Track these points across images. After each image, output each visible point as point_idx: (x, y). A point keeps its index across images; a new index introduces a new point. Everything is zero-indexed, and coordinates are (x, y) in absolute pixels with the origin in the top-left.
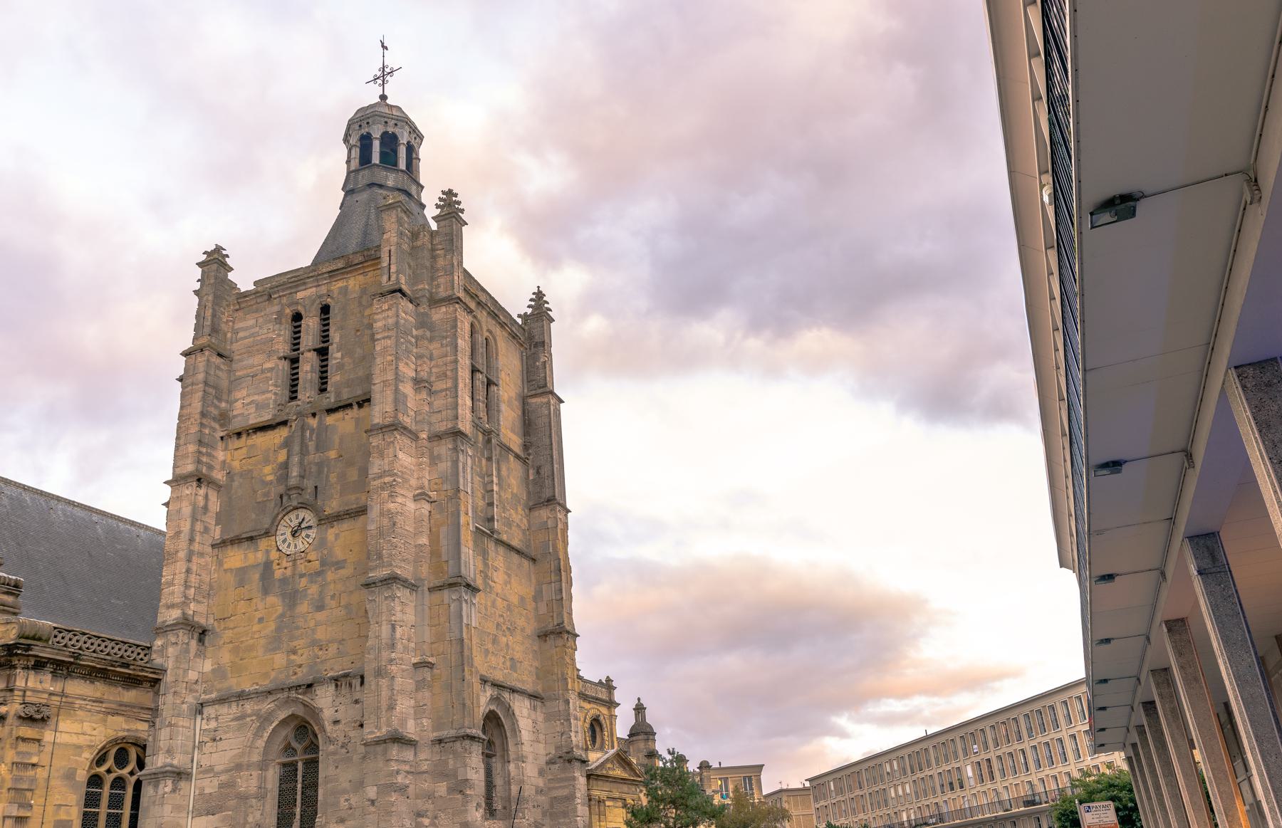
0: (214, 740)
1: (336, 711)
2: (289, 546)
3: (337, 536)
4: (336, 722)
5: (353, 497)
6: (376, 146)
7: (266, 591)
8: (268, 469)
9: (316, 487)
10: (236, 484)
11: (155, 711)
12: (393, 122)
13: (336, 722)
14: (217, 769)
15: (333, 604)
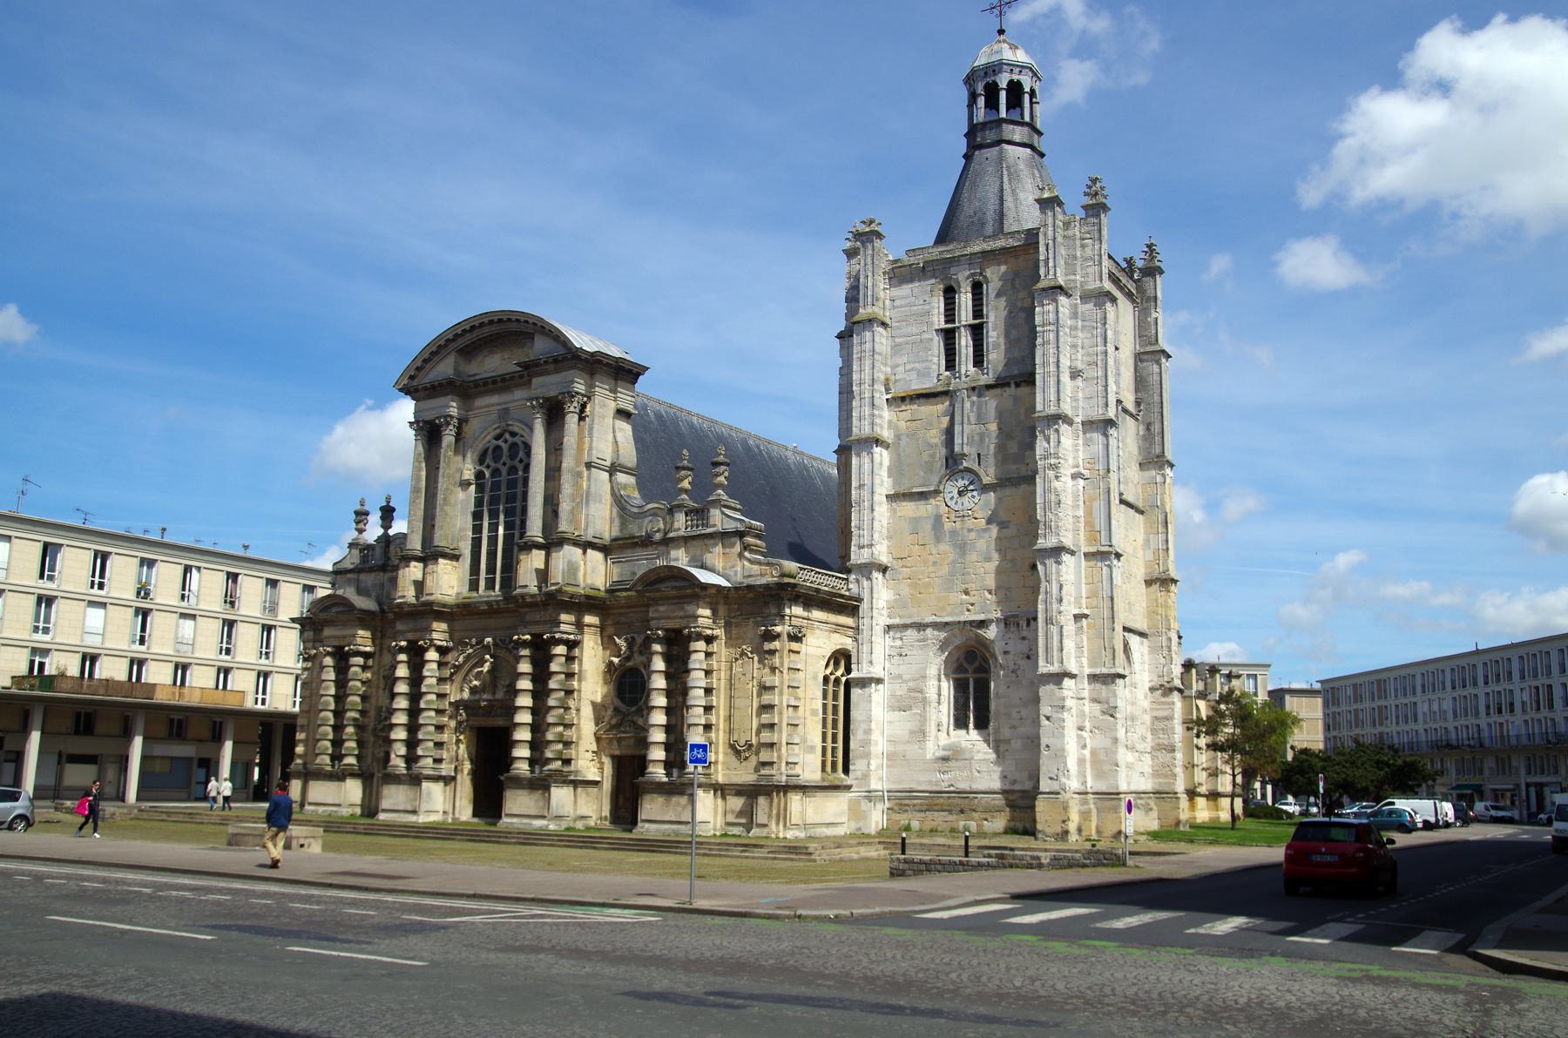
2: (956, 503)
4: (1006, 653)
5: (1014, 467)
6: (1003, 95)
7: (938, 539)
9: (979, 455)
10: (903, 443)
11: (857, 629)
12: (1018, 69)
14: (905, 677)
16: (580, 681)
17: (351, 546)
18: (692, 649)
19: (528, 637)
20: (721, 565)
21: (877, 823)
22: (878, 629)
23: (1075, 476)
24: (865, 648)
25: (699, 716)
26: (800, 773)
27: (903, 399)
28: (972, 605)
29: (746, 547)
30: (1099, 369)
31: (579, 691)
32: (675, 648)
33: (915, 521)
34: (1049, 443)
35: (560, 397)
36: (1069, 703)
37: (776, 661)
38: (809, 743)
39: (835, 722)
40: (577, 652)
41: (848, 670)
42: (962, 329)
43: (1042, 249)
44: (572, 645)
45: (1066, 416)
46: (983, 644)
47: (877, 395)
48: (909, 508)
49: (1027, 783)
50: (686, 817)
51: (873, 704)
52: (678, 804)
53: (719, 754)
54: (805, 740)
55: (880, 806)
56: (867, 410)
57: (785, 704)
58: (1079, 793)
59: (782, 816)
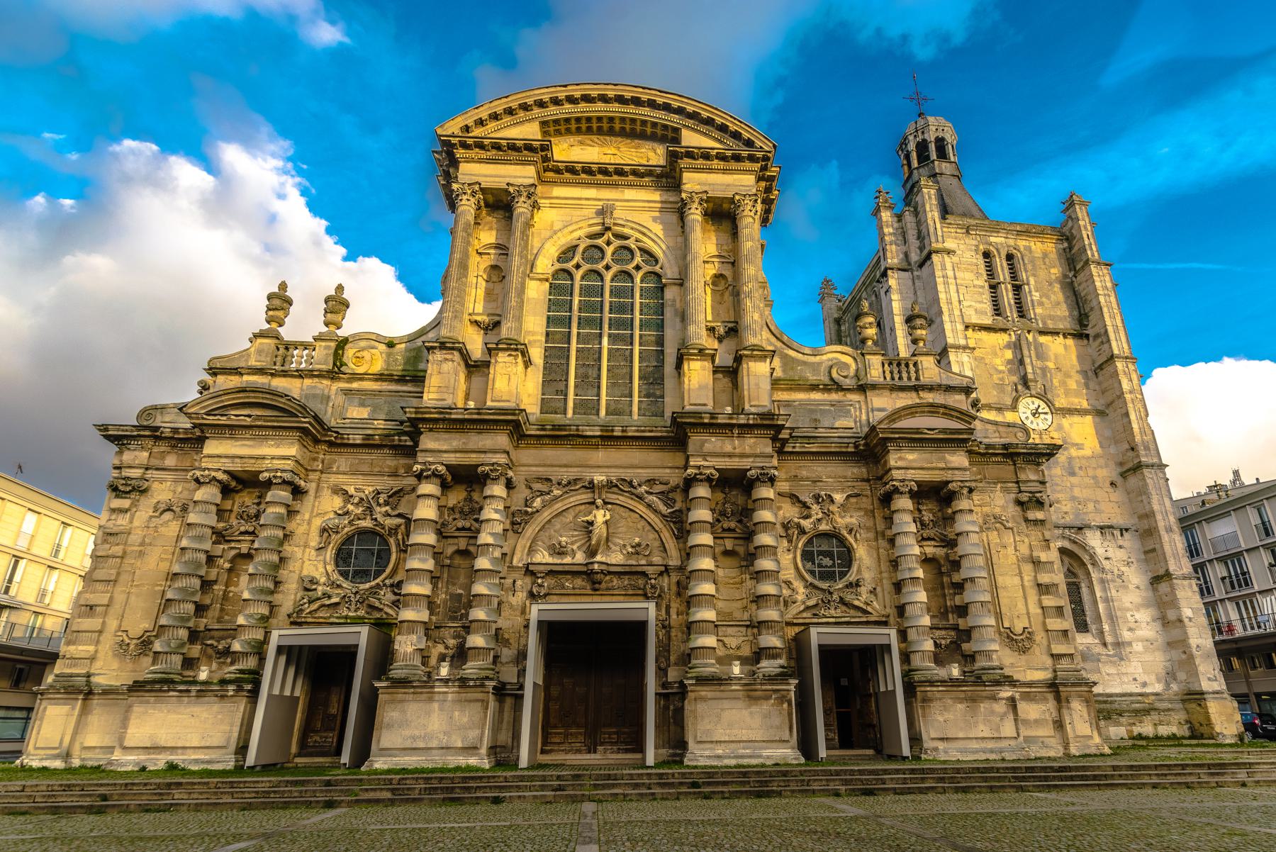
2: (1032, 422)
3: (1071, 425)
13: (1107, 559)
15: (1081, 473)
49: (1157, 685)
52: (993, 712)
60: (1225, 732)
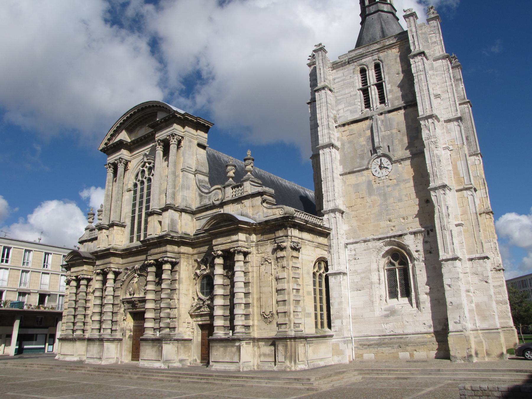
0: (355, 259)
1: (417, 246)
2: (379, 173)
3: (403, 168)
8: (362, 139)
11: (330, 246)
14: (359, 271)
16: (179, 284)
17: (86, 229)
18: (236, 259)
19: (152, 261)
20: (251, 213)
21: (349, 356)
22: (342, 245)
23: (445, 149)
24: (335, 256)
25: (242, 299)
26: (303, 329)
27: (344, 125)
28: (394, 227)
29: (264, 201)
30: (450, 94)
31: (179, 289)
32: (228, 261)
33: (356, 186)
34: (429, 131)
35: (168, 138)
36: (461, 276)
37: (285, 263)
38: (307, 311)
39: (321, 299)
40: (177, 268)
41: (327, 269)
42: (372, 87)
43: (410, 38)
44: (174, 264)
45: (436, 116)
46: (403, 247)
47: (330, 124)
48: (352, 179)
50: (236, 359)
51: (342, 287)
53: (255, 321)
54: (304, 309)
55: (350, 346)
56: (326, 131)
57: (291, 288)
58: (473, 330)
59: (293, 357)
60: (457, 355)
